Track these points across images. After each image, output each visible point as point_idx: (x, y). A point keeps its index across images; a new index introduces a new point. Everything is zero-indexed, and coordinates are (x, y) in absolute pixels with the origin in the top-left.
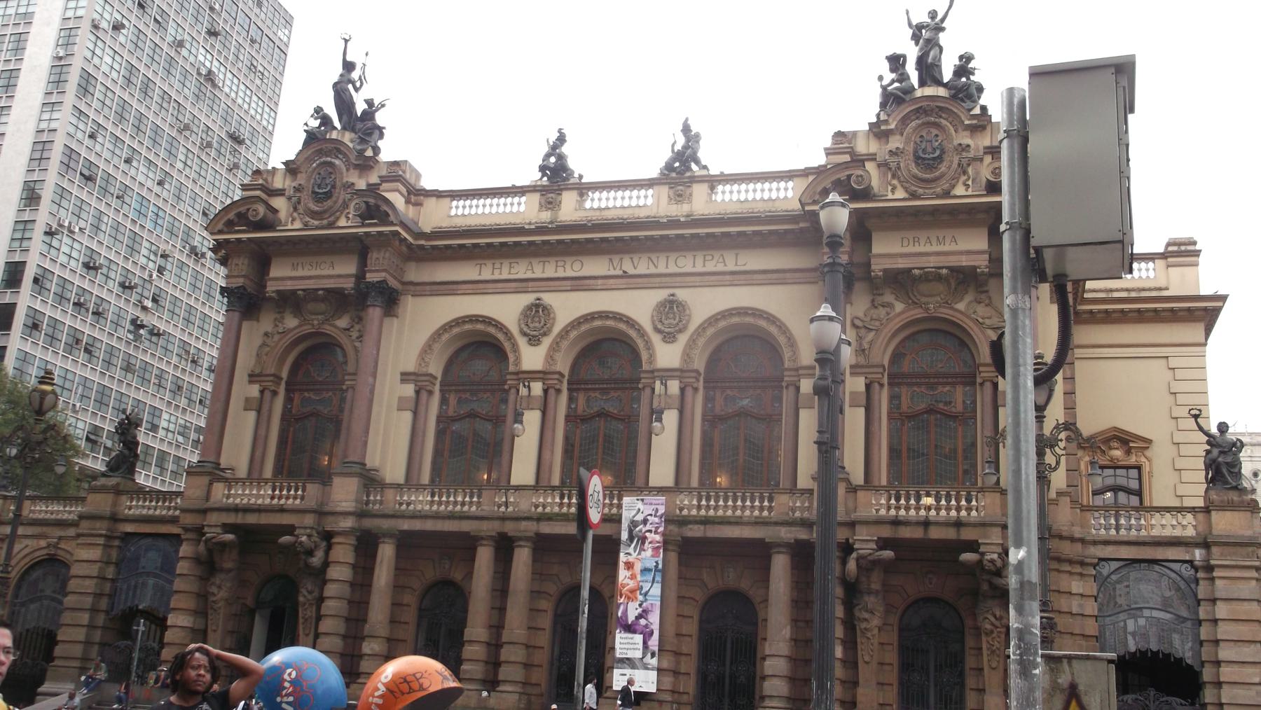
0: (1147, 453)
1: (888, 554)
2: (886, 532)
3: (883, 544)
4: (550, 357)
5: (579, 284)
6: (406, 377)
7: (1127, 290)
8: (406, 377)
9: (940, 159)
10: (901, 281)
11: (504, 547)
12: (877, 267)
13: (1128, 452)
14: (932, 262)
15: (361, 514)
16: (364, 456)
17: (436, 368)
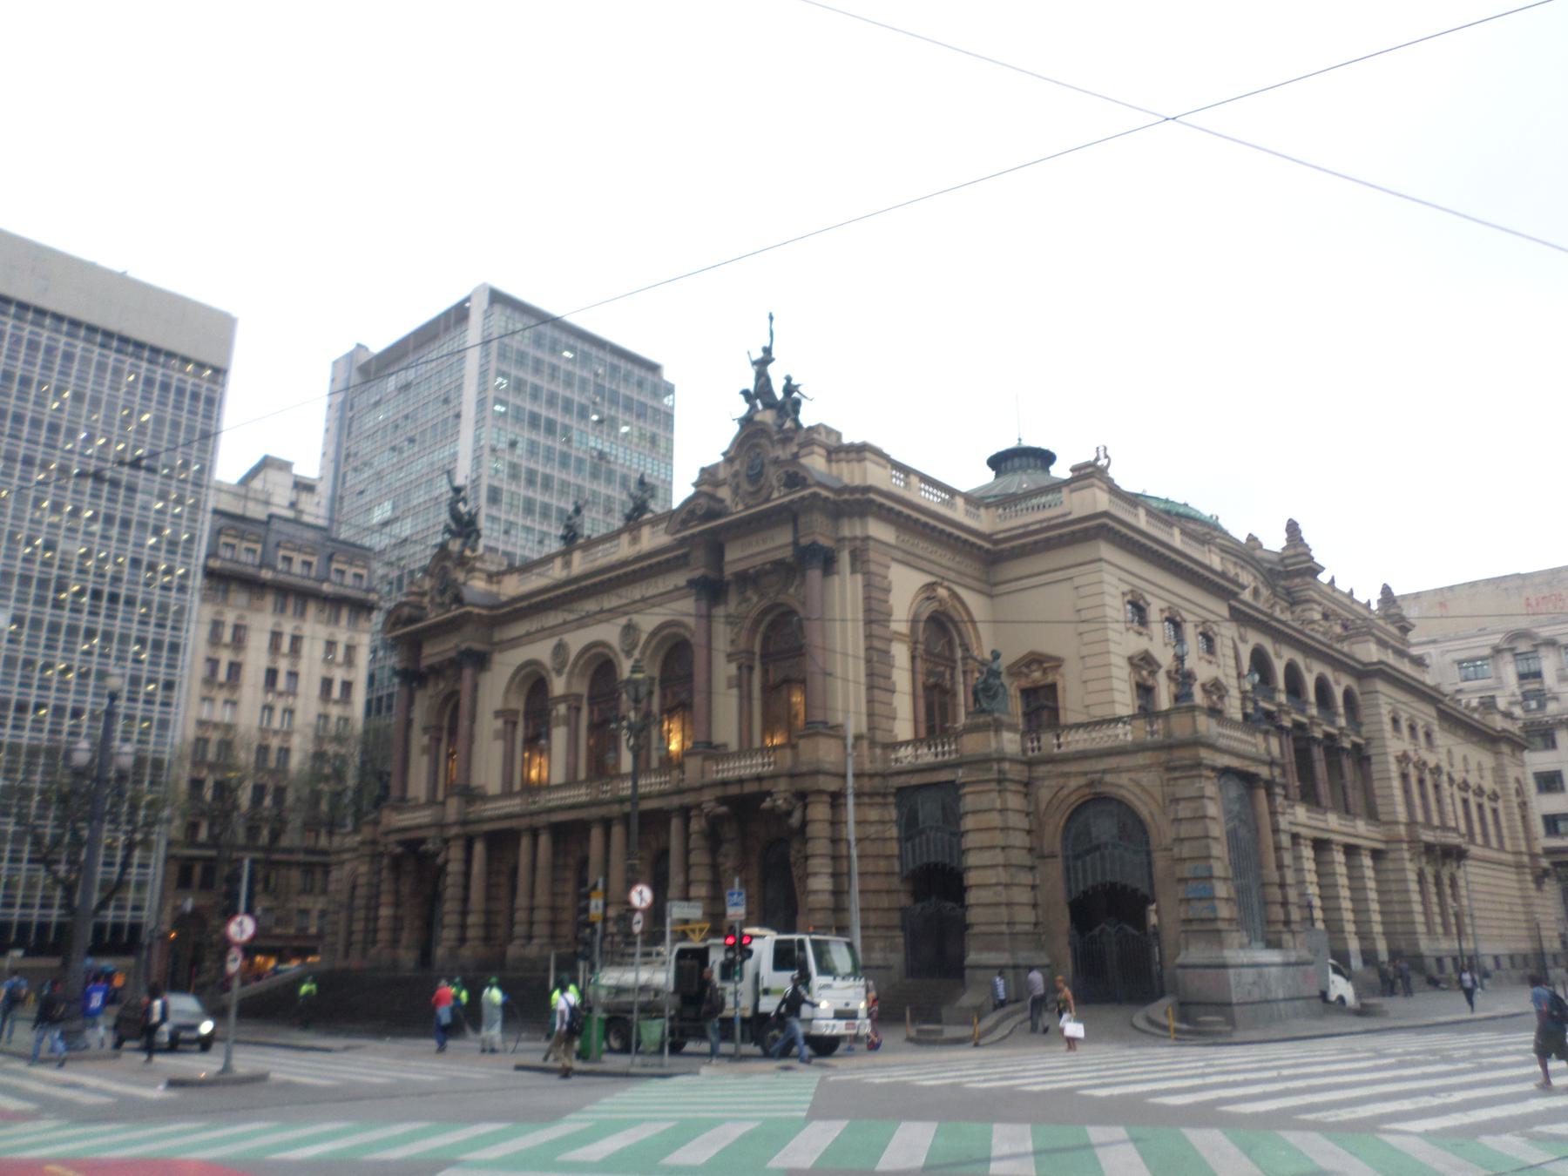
0: (1061, 670)
1: (723, 809)
2: (719, 792)
3: (722, 800)
4: (569, 684)
5: (581, 623)
6: (498, 714)
7: (1040, 522)
8: (498, 714)
9: (760, 474)
10: (746, 579)
11: (535, 833)
13: (1045, 671)
14: (758, 561)
15: (464, 823)
16: (468, 777)
17: (518, 704)
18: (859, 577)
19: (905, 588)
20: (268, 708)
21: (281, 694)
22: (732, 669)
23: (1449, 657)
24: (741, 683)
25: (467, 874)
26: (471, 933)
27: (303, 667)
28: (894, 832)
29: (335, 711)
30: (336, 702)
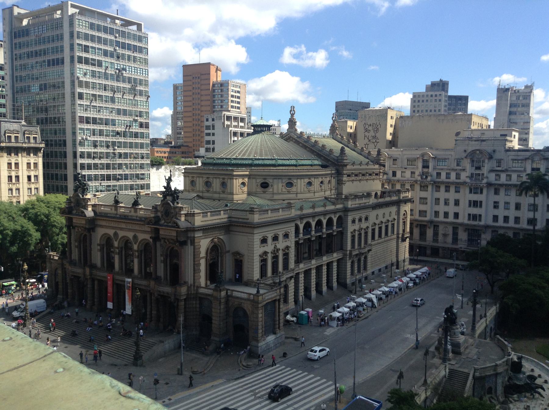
5: (121, 229)
6: (98, 245)
8: (98, 245)
12: (161, 236)
18: (192, 247)
19: (204, 244)
20: (11, 190)
21: (14, 184)
22: (162, 258)
23: (405, 157)
24: (165, 262)
25: (93, 287)
26: (96, 303)
27: (20, 174)
28: (198, 306)
29: (33, 186)
30: (33, 183)
